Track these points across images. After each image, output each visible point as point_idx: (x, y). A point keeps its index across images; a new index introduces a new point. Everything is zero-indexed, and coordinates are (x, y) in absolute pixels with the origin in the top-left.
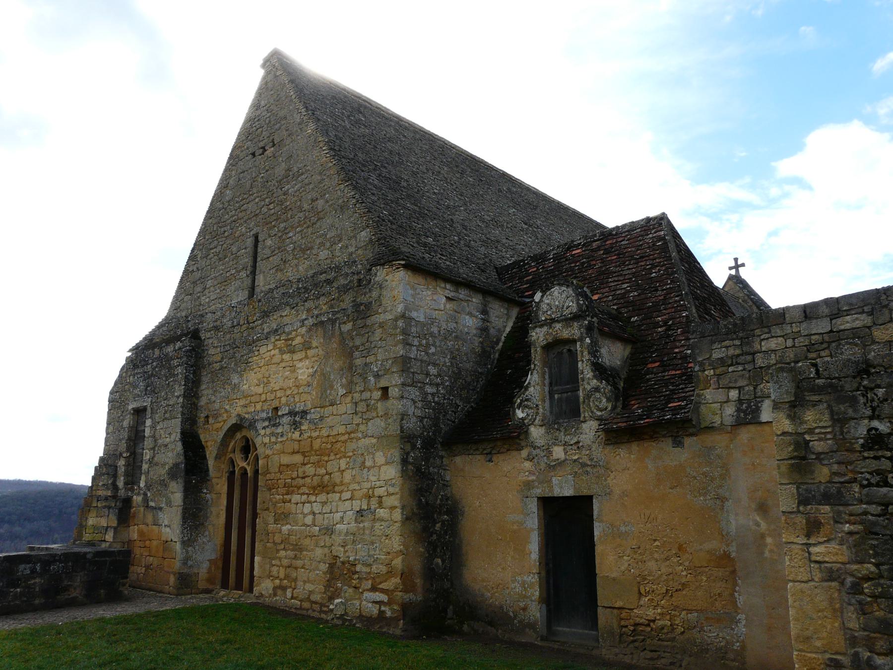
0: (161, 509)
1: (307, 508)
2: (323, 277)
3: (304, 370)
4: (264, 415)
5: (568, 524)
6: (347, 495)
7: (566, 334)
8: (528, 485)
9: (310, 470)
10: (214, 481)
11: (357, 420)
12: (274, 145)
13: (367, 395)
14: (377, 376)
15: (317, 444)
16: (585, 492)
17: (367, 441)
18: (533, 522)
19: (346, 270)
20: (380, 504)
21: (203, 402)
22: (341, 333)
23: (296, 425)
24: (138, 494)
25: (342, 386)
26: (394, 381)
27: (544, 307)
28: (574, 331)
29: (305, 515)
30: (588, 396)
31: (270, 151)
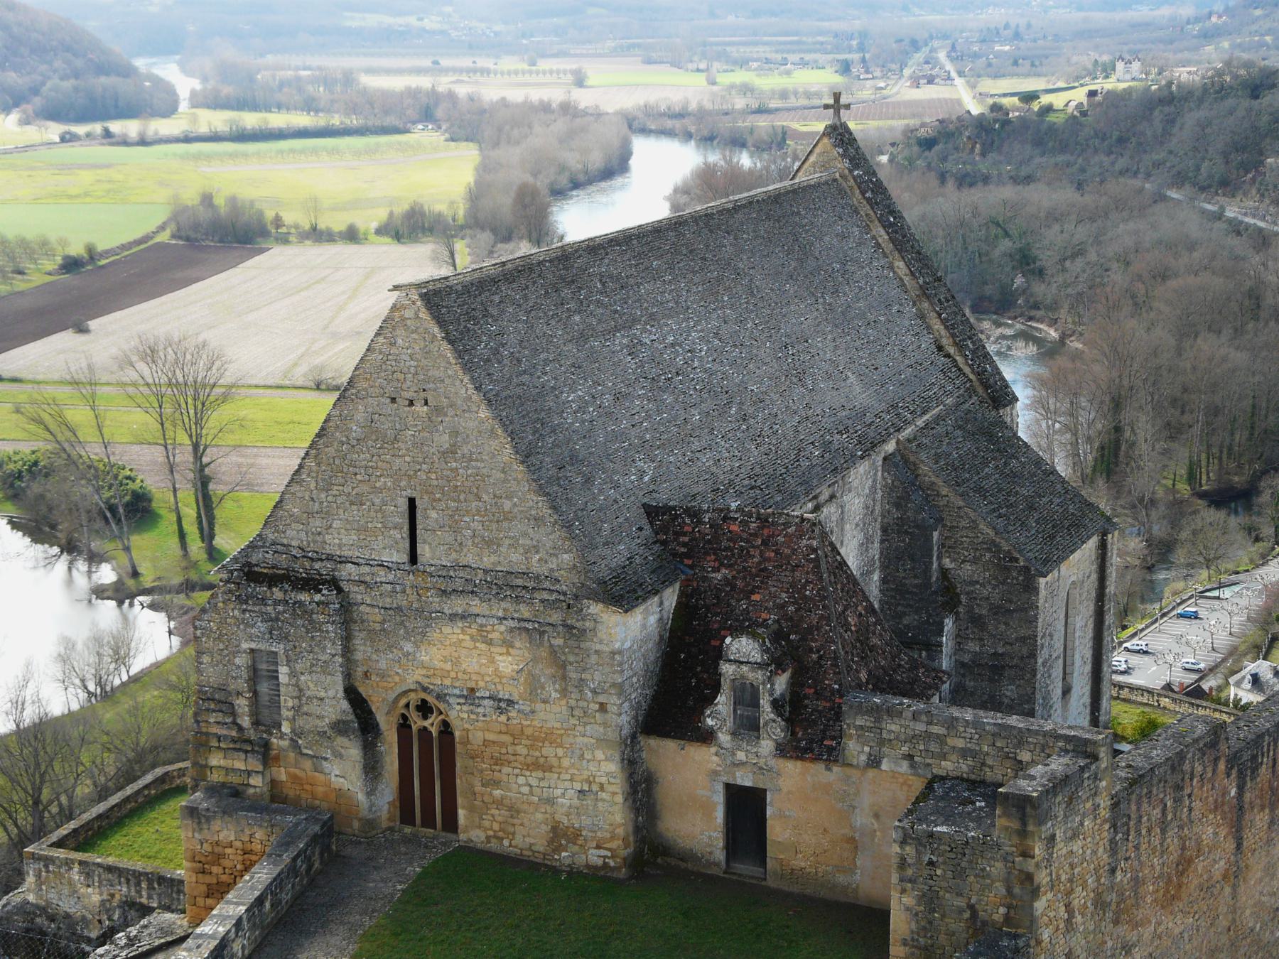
0: (326, 759)
1: (521, 780)
2: (519, 582)
3: (507, 664)
4: (457, 692)
11: (573, 721)
14: (594, 692)
15: (529, 731)
17: (586, 740)
19: (547, 585)
23: (501, 711)
25: (556, 691)
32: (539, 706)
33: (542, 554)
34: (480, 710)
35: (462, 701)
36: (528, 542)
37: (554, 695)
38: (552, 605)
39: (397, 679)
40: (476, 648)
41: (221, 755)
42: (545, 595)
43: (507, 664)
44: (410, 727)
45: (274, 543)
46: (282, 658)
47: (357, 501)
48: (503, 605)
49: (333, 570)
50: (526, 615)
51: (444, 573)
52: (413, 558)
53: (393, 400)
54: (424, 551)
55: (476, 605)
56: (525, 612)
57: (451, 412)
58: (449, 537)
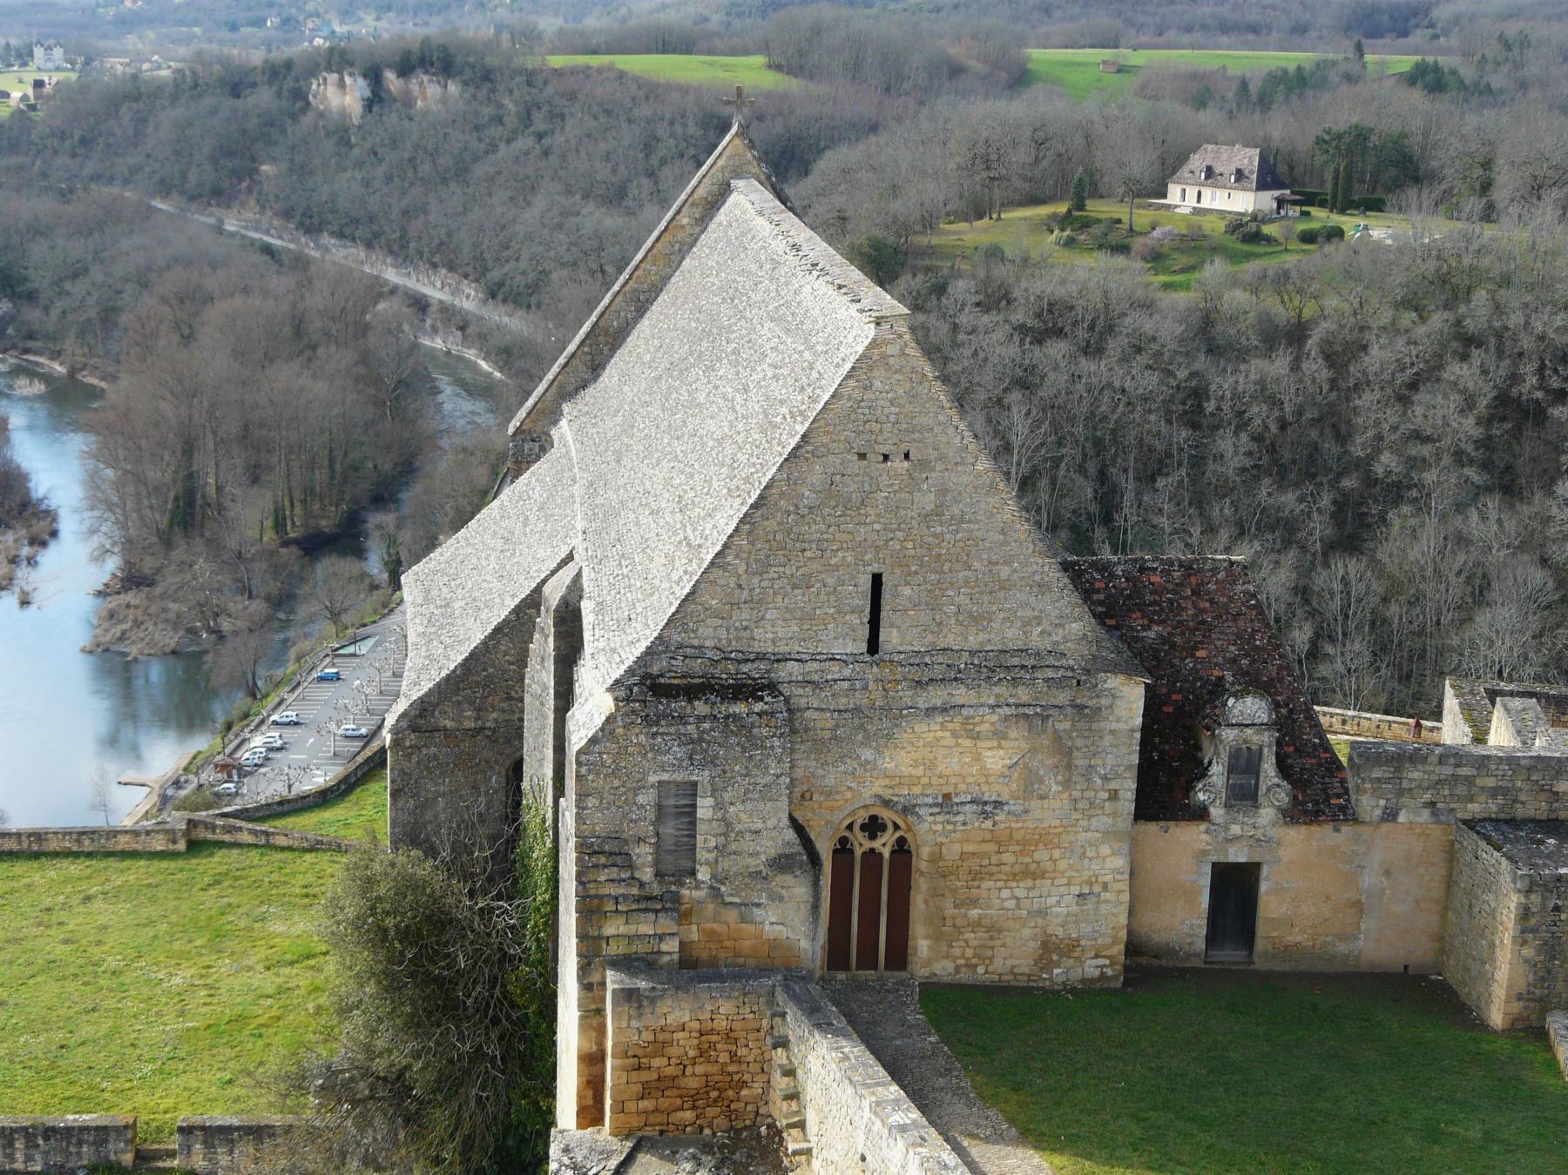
0: (758, 905)
1: (1005, 893)
2: (1016, 661)
3: (996, 759)
4: (930, 800)
6: (1065, 881)
9: (1008, 858)
11: (1076, 816)
14: (1105, 778)
15: (1018, 835)
17: (1089, 835)
19: (1051, 661)
23: (985, 815)
24: (697, 888)
25: (1057, 783)
32: (1034, 804)
33: (1045, 625)
34: (960, 818)
35: (936, 810)
36: (1029, 613)
37: (1055, 788)
38: (1059, 683)
39: (849, 795)
40: (958, 745)
41: (622, 920)
42: (1050, 673)
43: (996, 759)
44: (851, 852)
45: (680, 646)
47: (804, 584)
48: (996, 690)
49: (768, 672)
50: (1025, 698)
51: (918, 660)
52: (873, 646)
53: (862, 456)
54: (890, 637)
55: (960, 694)
56: (1023, 694)
57: (939, 466)
58: (924, 617)
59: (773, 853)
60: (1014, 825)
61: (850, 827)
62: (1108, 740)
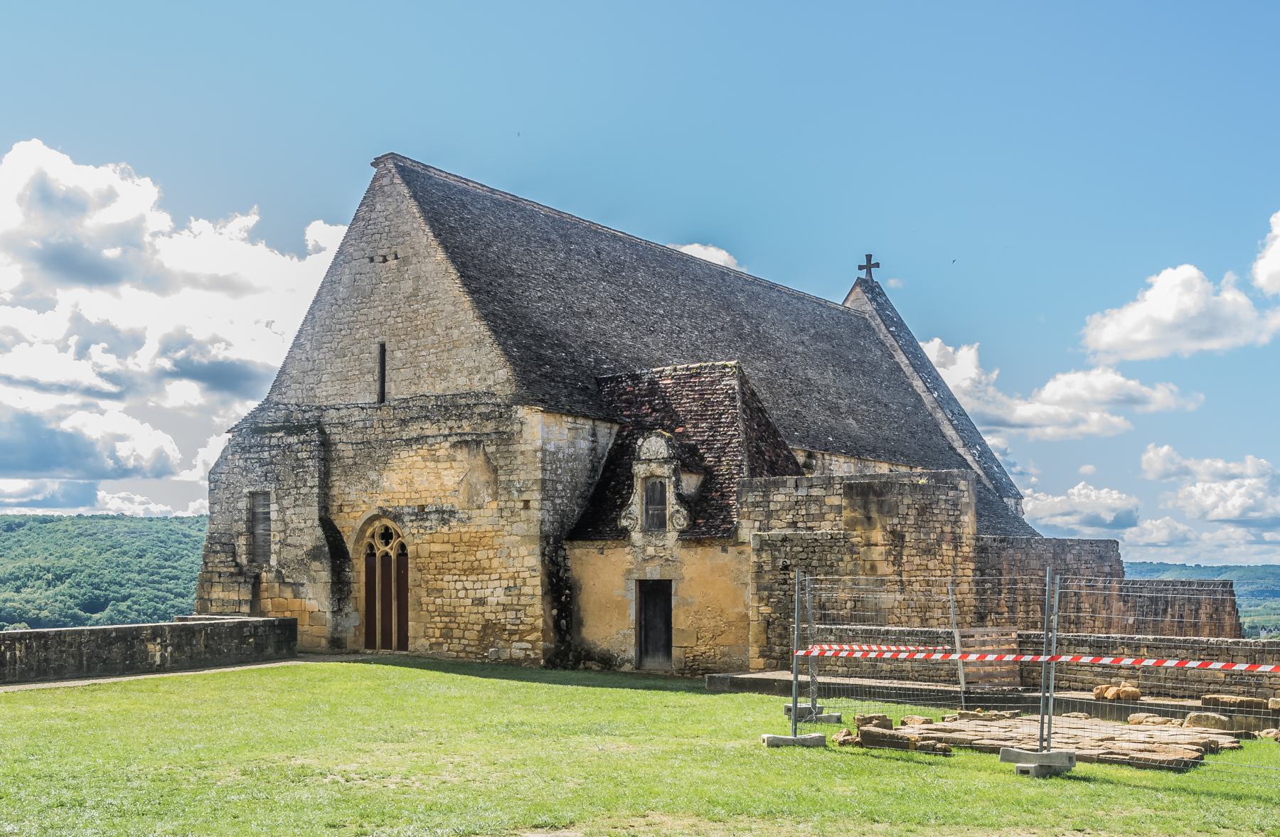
0: (303, 585)
2: (463, 402)
3: (450, 477)
5: (655, 597)
7: (659, 471)
8: (629, 571)
9: (460, 557)
10: (354, 561)
11: (502, 522)
12: (396, 258)
13: (510, 504)
14: (520, 491)
15: (466, 538)
16: (667, 578)
18: (632, 596)
19: (485, 400)
20: (525, 584)
21: (335, 491)
22: (486, 454)
23: (445, 522)
24: (270, 571)
26: (535, 496)
27: (644, 449)
28: (666, 470)
29: (458, 591)
30: (672, 516)
31: (392, 263)
32: (475, 513)
33: (483, 374)
34: (428, 524)
36: (472, 364)
37: (488, 499)
38: (486, 417)
39: (364, 507)
45: (277, 404)
46: (273, 497)
48: (450, 423)
50: (467, 429)
52: (382, 397)
53: (372, 260)
54: (391, 388)
55: (430, 429)
57: (414, 260)
59: (310, 545)
60: (463, 530)
61: (373, 536)
62: (520, 459)
